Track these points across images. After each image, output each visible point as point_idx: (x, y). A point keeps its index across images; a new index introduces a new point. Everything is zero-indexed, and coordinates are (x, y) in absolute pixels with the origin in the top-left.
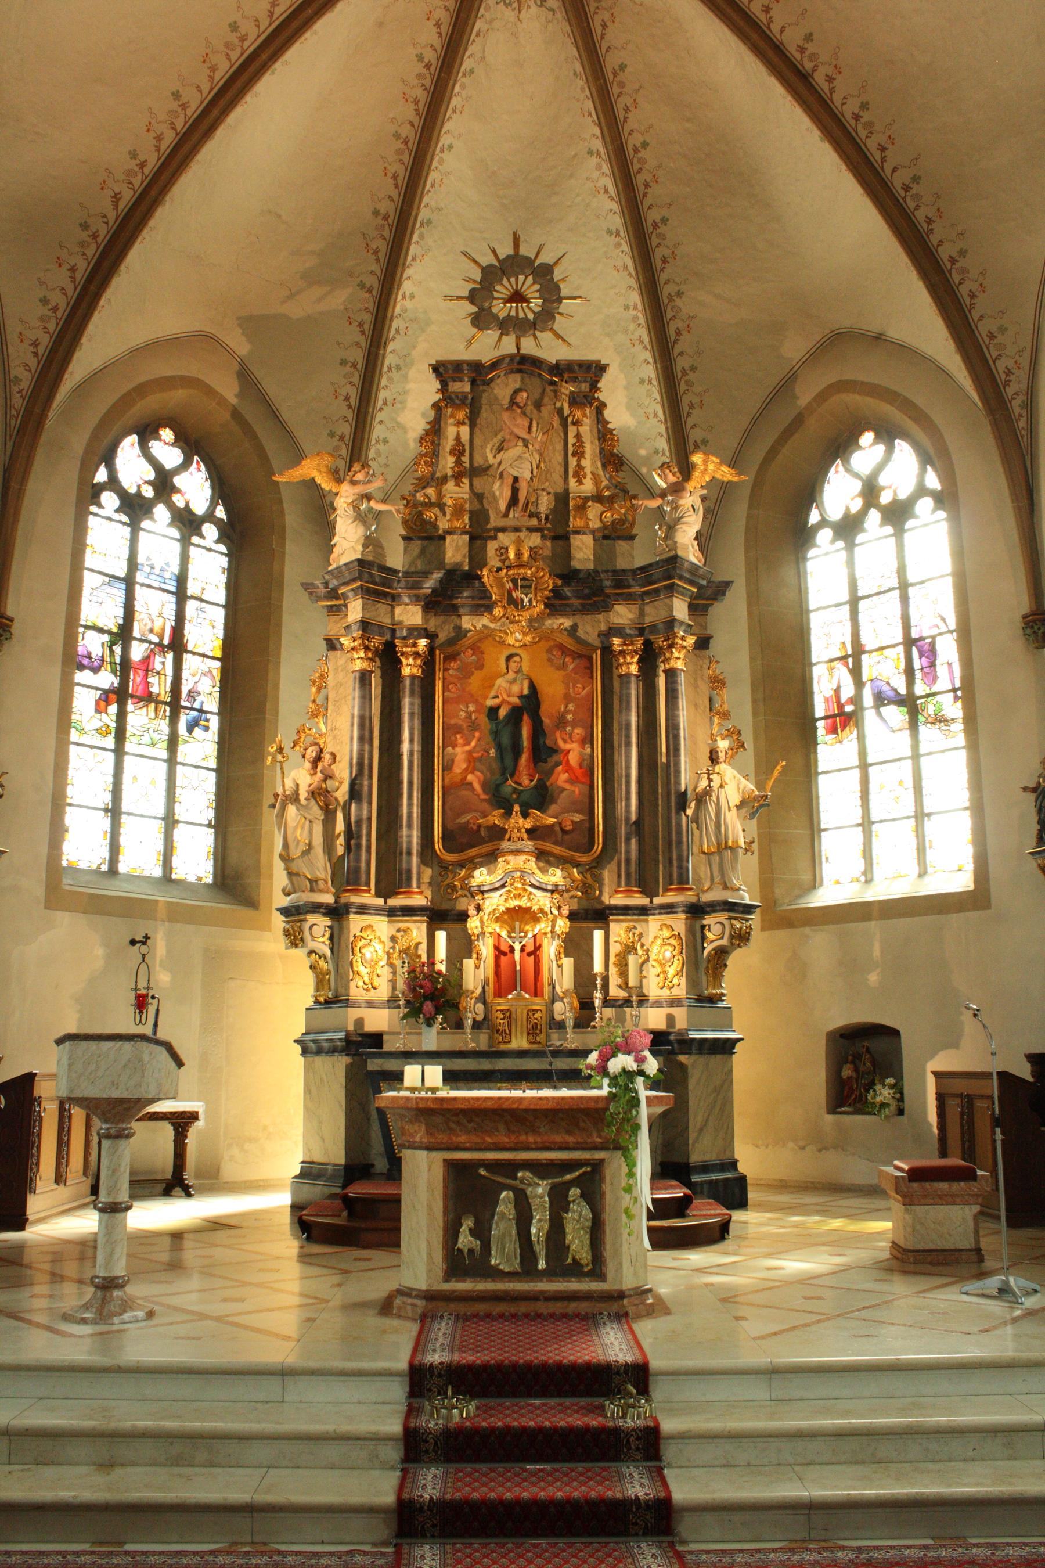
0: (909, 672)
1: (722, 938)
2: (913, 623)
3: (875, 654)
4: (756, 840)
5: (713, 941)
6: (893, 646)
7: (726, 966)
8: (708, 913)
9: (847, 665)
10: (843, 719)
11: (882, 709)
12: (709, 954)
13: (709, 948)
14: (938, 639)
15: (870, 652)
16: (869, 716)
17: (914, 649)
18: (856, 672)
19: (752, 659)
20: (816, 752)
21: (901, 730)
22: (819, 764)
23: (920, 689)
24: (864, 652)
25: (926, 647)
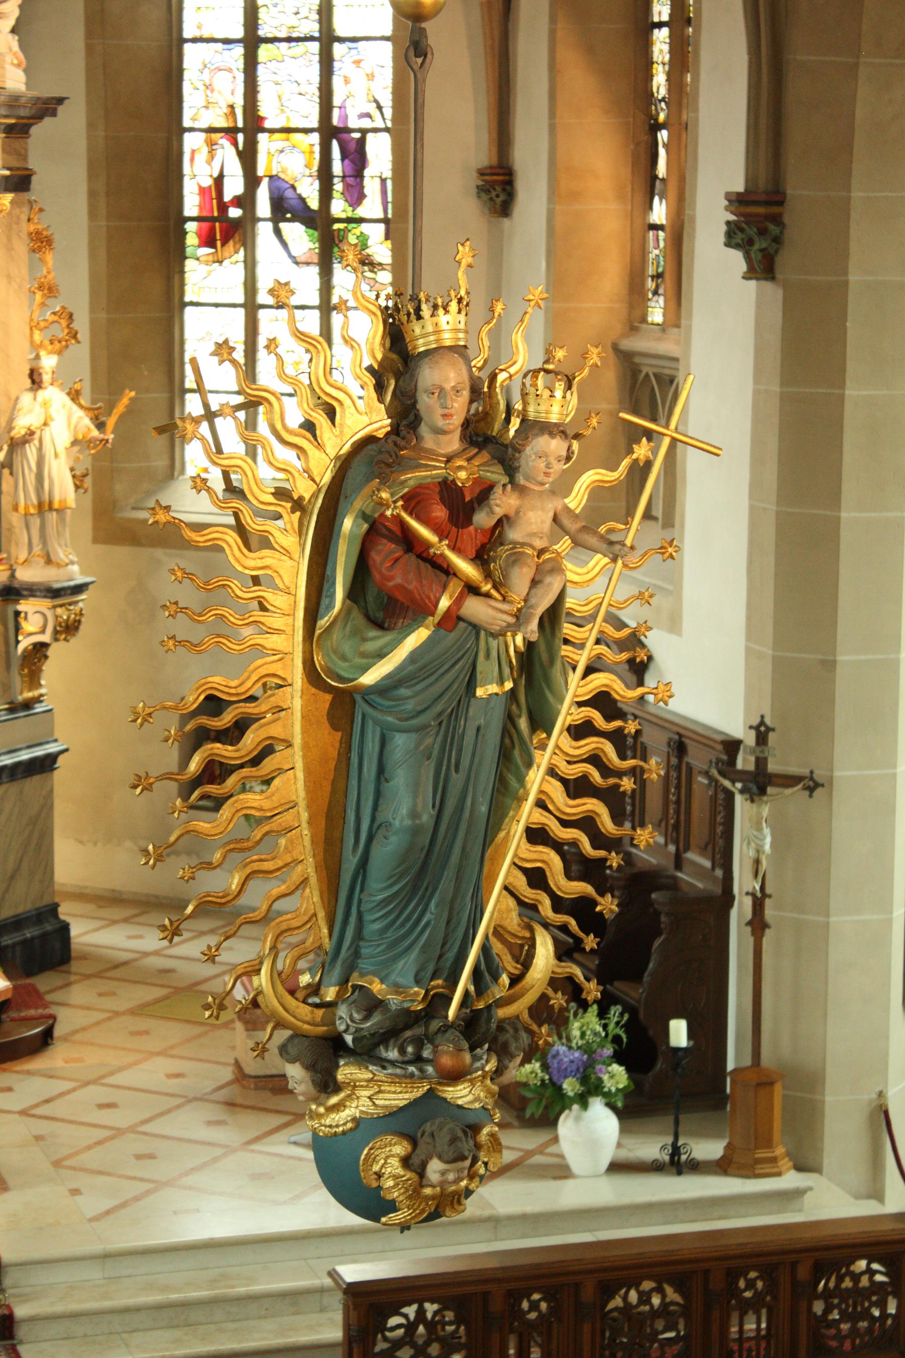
0: (325, 175)
1: (43, 632)
2: (337, 101)
3: (277, 136)
4: (90, 472)
5: (31, 634)
6: (306, 131)
7: (46, 657)
8: (25, 597)
9: (235, 143)
10: (228, 229)
11: (283, 226)
12: (25, 650)
13: (25, 643)
14: (370, 136)
15: (272, 131)
16: (264, 230)
17: (335, 145)
18: (248, 157)
19: (91, 125)
20: (182, 272)
21: (308, 264)
22: (188, 288)
23: (339, 207)
24: (264, 130)
25: (352, 146)
